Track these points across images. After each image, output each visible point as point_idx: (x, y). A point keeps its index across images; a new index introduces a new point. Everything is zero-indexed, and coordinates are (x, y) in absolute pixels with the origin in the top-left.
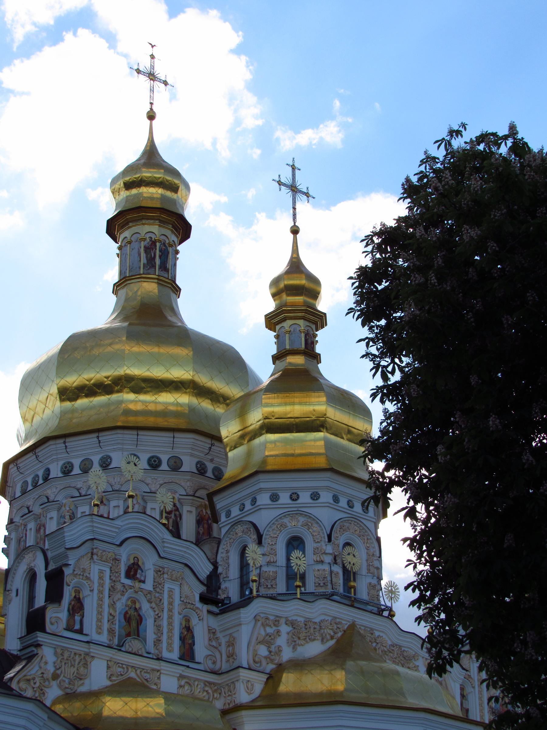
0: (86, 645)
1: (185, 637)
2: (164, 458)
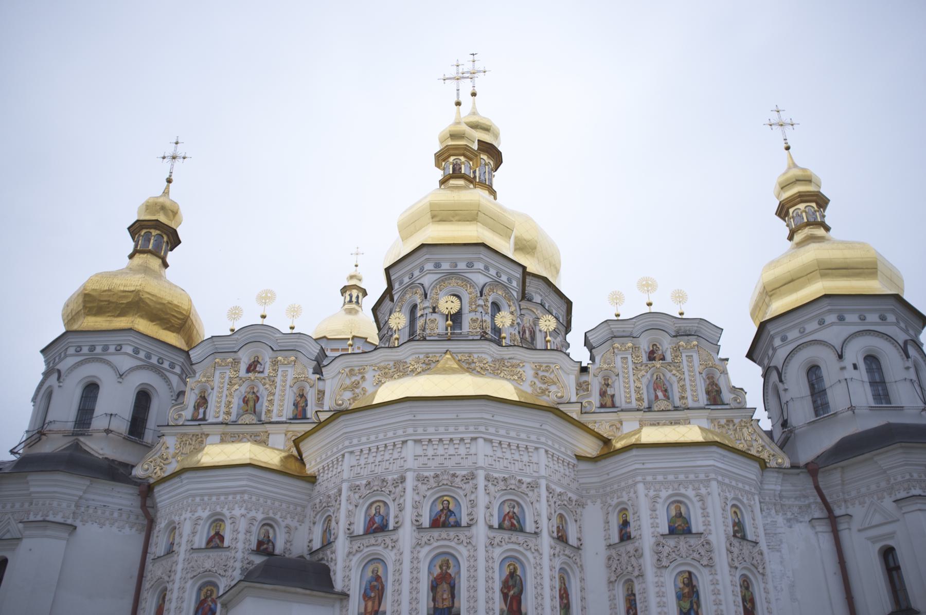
0: (198, 428)
1: (298, 403)
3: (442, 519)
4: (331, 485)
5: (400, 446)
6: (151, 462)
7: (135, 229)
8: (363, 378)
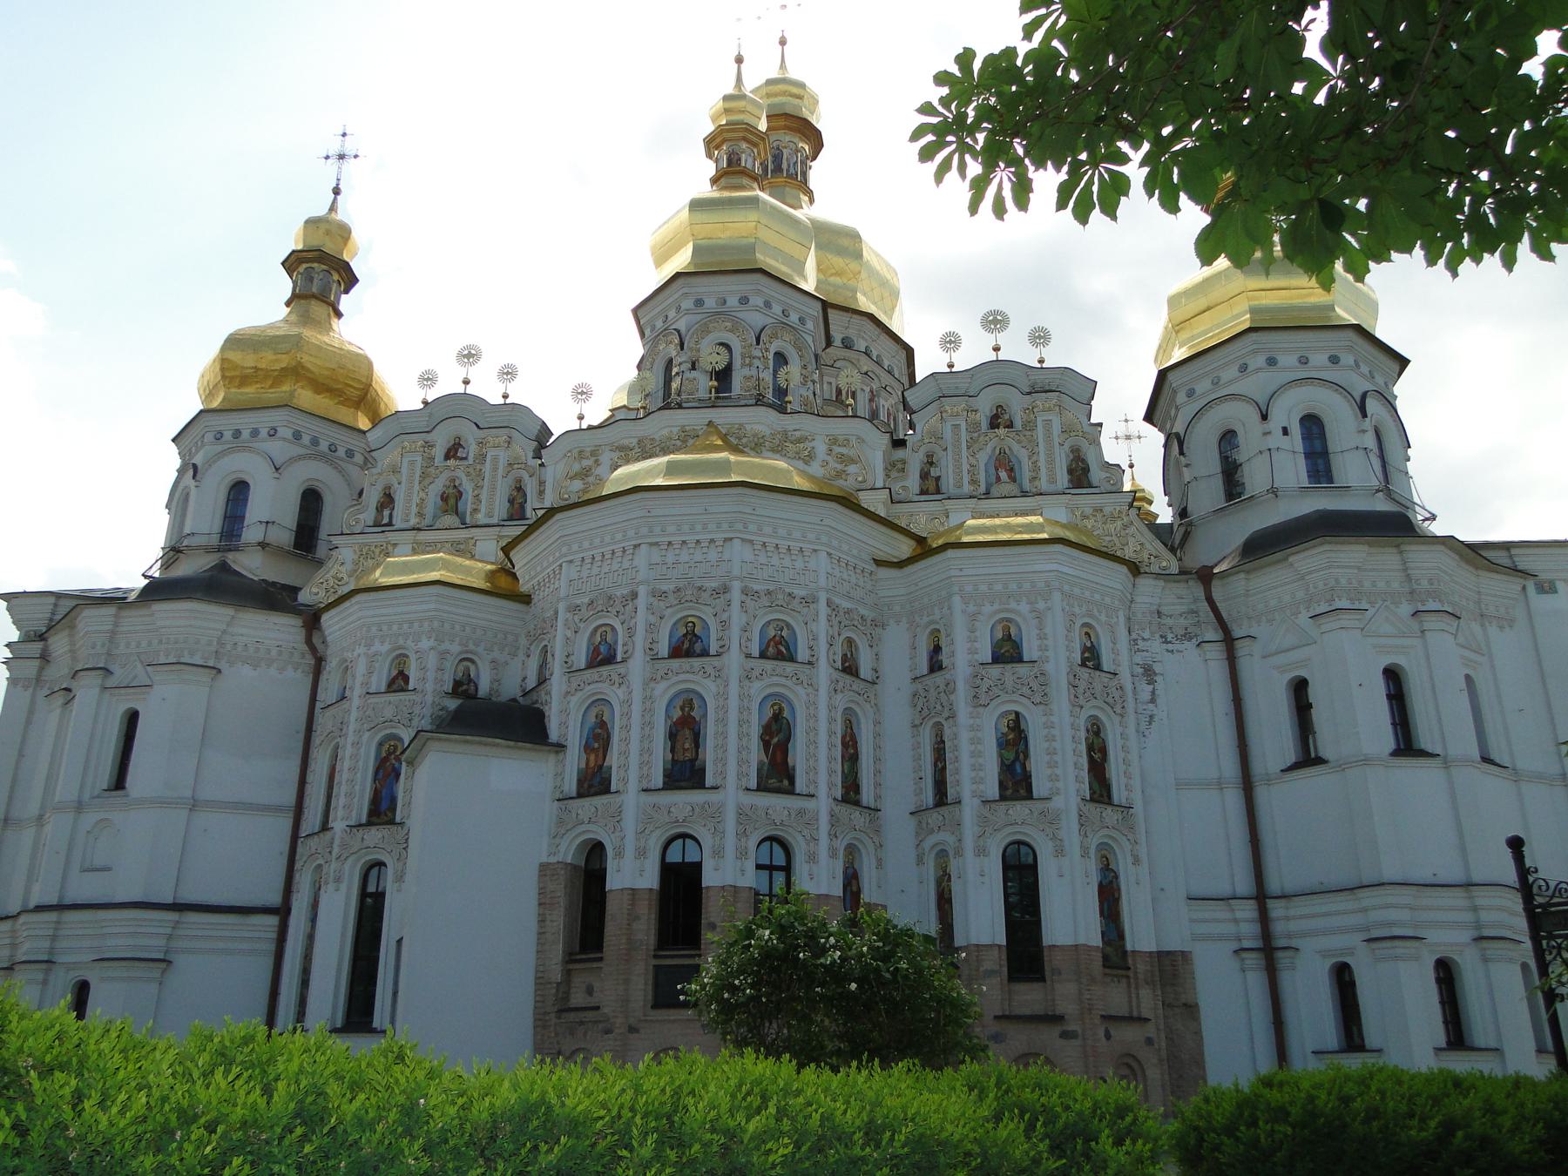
3: (686, 646)
5: (631, 551)
6: (322, 583)
7: (292, 263)
8: (596, 461)
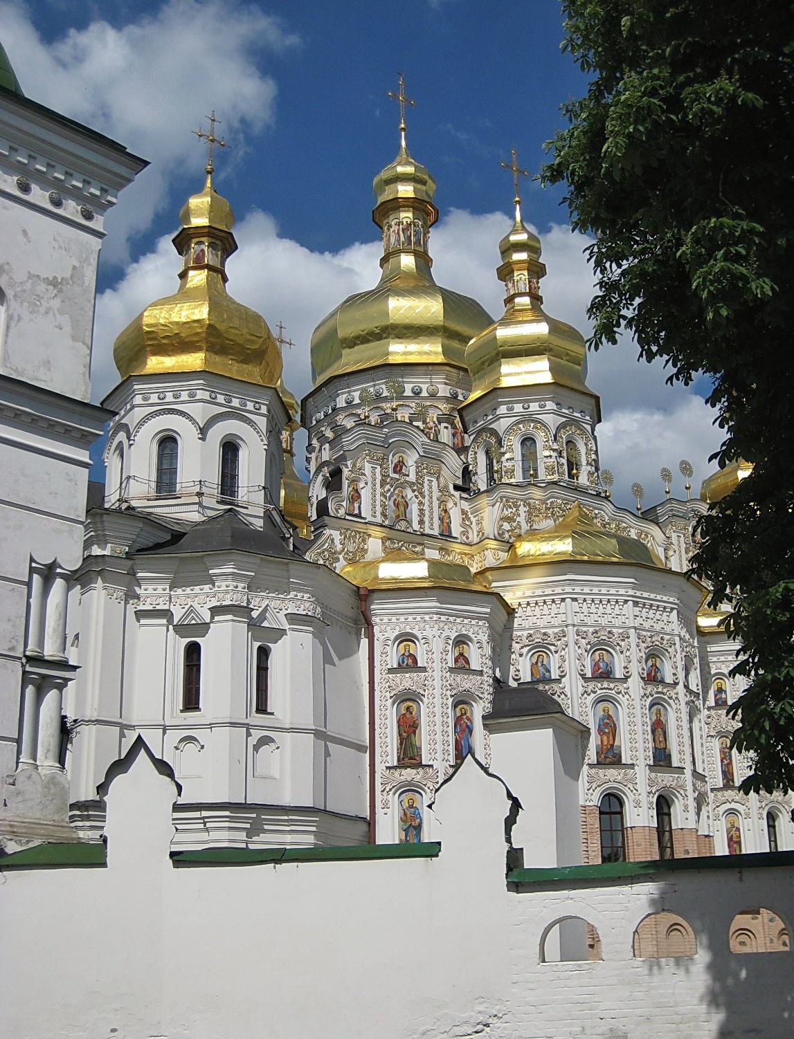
1: (443, 518)
2: (424, 387)
3: (653, 674)
4: (541, 623)
